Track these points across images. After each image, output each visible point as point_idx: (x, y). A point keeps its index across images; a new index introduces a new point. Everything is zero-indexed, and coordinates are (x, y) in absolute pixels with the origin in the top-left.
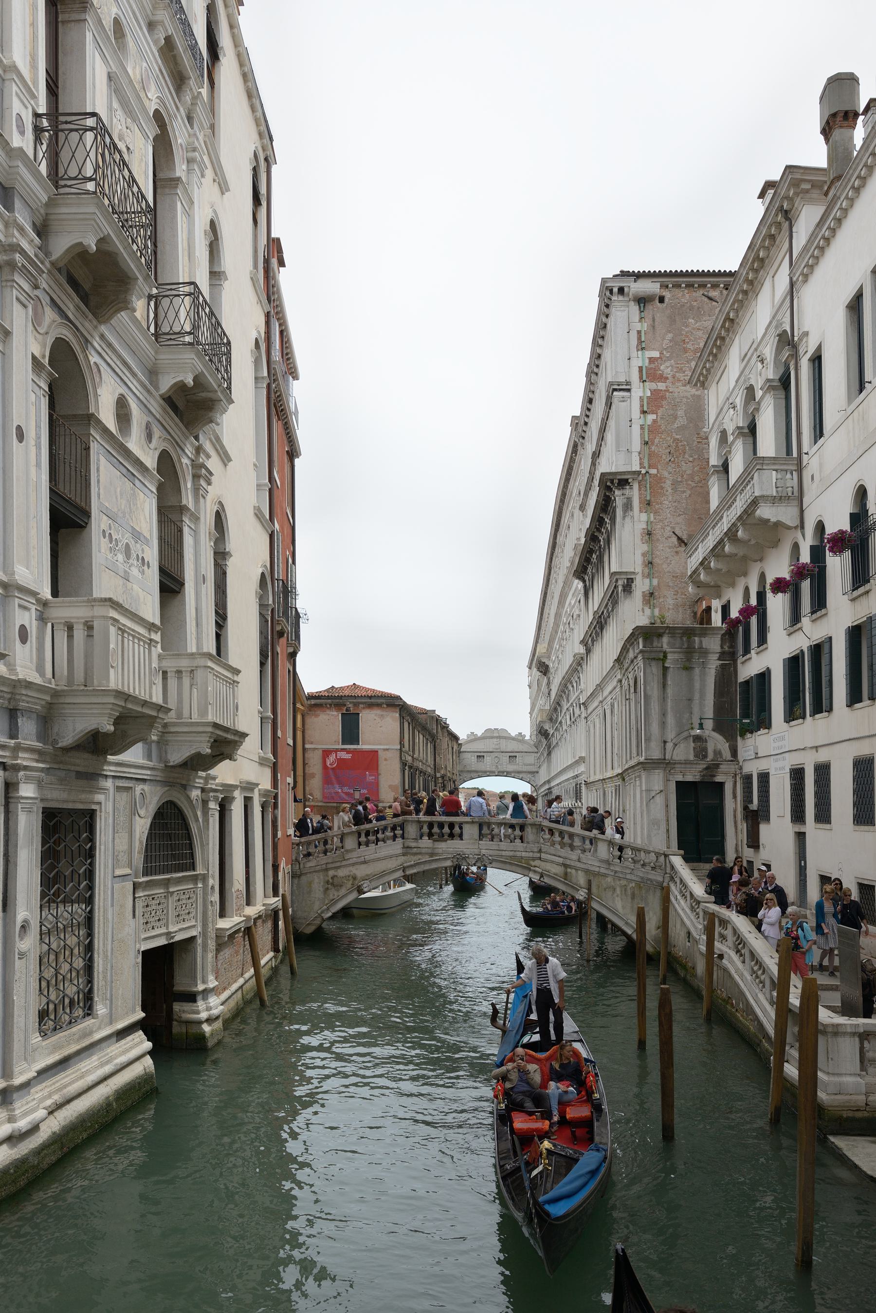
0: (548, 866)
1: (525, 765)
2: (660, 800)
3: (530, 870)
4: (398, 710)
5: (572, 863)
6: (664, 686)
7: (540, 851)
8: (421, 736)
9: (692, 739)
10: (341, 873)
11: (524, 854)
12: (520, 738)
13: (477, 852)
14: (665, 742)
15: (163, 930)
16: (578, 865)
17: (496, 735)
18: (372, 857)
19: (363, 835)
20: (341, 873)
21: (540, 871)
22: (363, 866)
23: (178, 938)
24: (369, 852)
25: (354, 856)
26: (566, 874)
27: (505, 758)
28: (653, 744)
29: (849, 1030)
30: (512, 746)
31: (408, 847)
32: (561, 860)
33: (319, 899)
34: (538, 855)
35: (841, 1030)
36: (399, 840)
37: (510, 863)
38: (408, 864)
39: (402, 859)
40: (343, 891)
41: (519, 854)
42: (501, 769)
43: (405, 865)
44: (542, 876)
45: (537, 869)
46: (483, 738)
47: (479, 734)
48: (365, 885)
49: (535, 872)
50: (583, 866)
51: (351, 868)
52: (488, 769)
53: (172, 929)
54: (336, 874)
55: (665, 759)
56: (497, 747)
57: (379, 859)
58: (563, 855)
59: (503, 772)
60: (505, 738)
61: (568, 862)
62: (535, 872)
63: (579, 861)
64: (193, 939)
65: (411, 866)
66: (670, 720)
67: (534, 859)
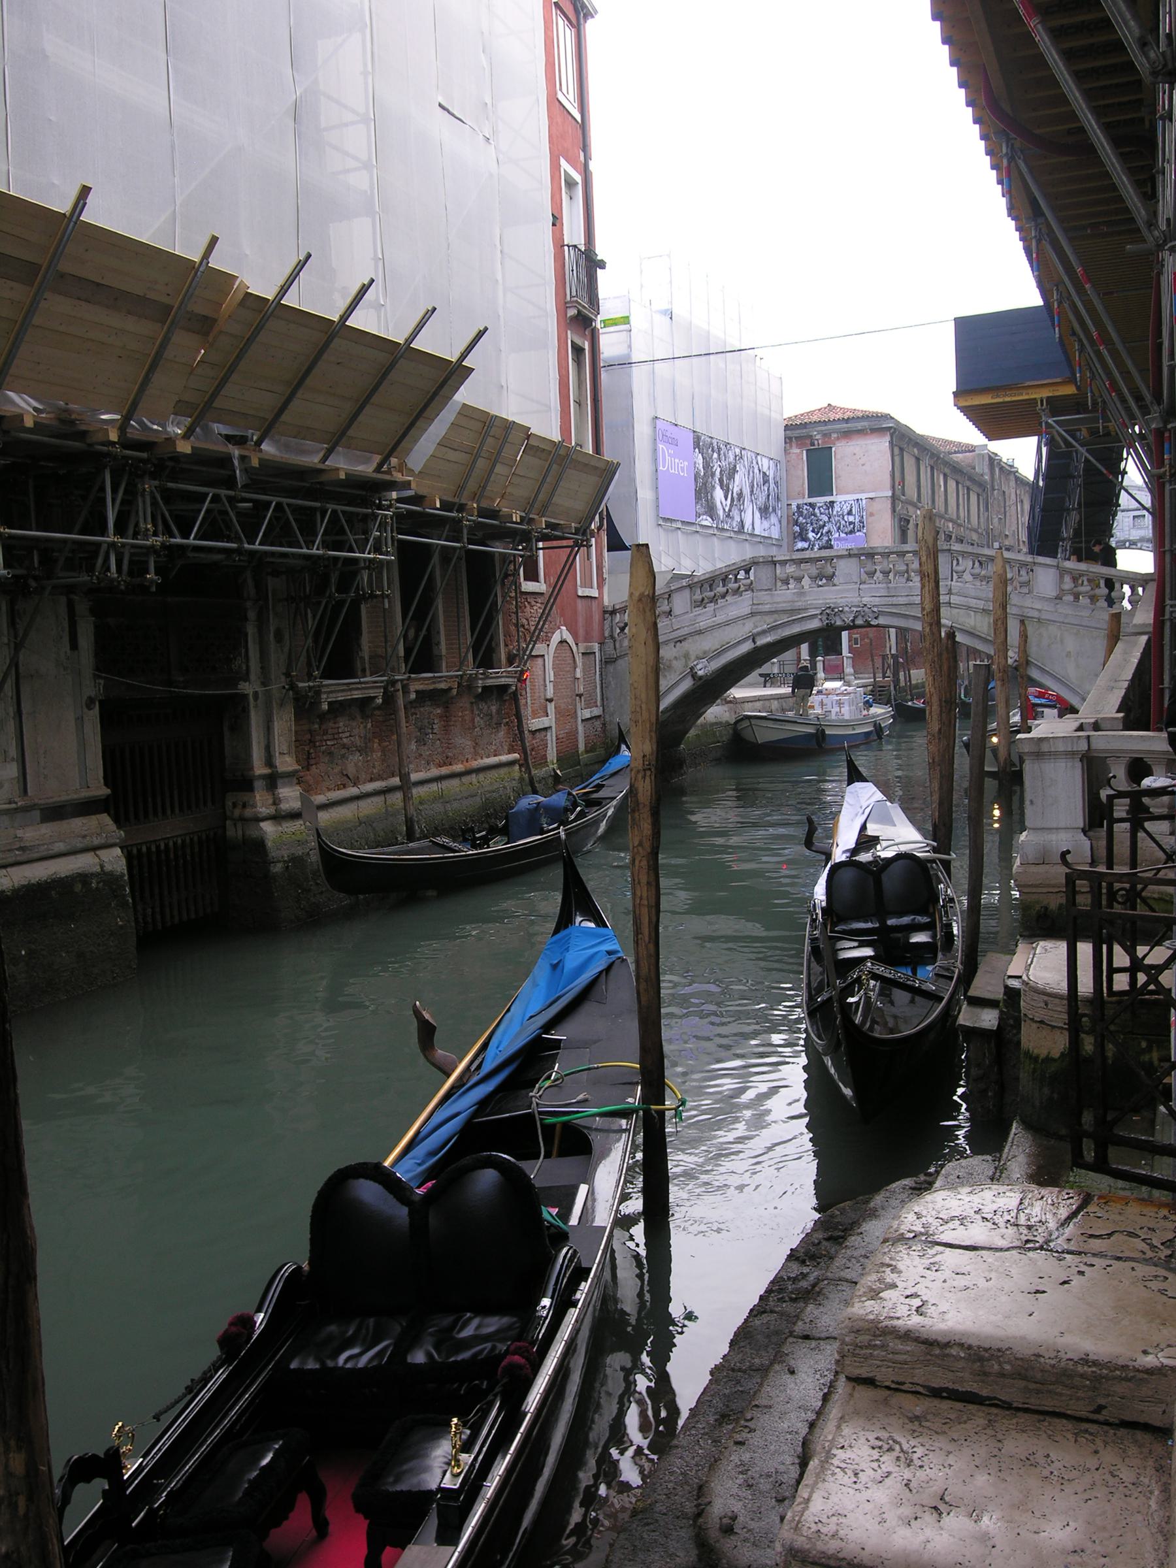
4: (888, 438)
8: (952, 484)
13: (856, 601)
18: (710, 622)
29: (1061, 748)
35: (1045, 748)
38: (759, 629)
43: (755, 631)
48: (699, 667)
57: (720, 626)
65: (764, 632)
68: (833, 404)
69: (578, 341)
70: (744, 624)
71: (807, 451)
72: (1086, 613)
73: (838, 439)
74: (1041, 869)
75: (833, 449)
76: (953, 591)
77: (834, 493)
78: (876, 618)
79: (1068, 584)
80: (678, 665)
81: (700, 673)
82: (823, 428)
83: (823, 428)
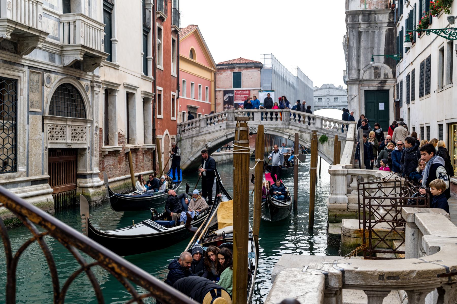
1: (342, 102)
2: (356, 100)
3: (284, 134)
6: (359, 42)
7: (289, 124)
9: (373, 68)
11: (281, 126)
12: (340, 88)
14: (359, 70)
17: (328, 87)
18: (213, 130)
19: (209, 120)
20: (200, 138)
21: (288, 134)
22: (208, 135)
24: (211, 128)
25: (204, 131)
27: (332, 99)
28: (353, 72)
30: (336, 93)
33: (189, 152)
34: (287, 127)
35: (337, 173)
36: (225, 122)
37: (275, 131)
39: (226, 131)
41: (279, 126)
42: (330, 104)
43: (227, 134)
44: (289, 136)
46: (321, 89)
47: (320, 87)
48: (209, 144)
49: (286, 135)
51: (203, 136)
52: (324, 105)
54: (197, 139)
55: (359, 79)
56: (328, 93)
57: (215, 131)
58: (299, 126)
59: (331, 106)
60: (333, 88)
62: (286, 135)
63: (307, 129)
64: (85, 149)
65: (230, 134)
66: (362, 59)
67: (286, 129)
68: (242, 57)
69: (174, 38)
71: (234, 73)
73: (244, 69)
74: (335, 204)
75: (242, 73)
77: (242, 87)
78: (266, 131)
80: (202, 144)
81: (209, 146)
82: (239, 66)
83: (239, 66)
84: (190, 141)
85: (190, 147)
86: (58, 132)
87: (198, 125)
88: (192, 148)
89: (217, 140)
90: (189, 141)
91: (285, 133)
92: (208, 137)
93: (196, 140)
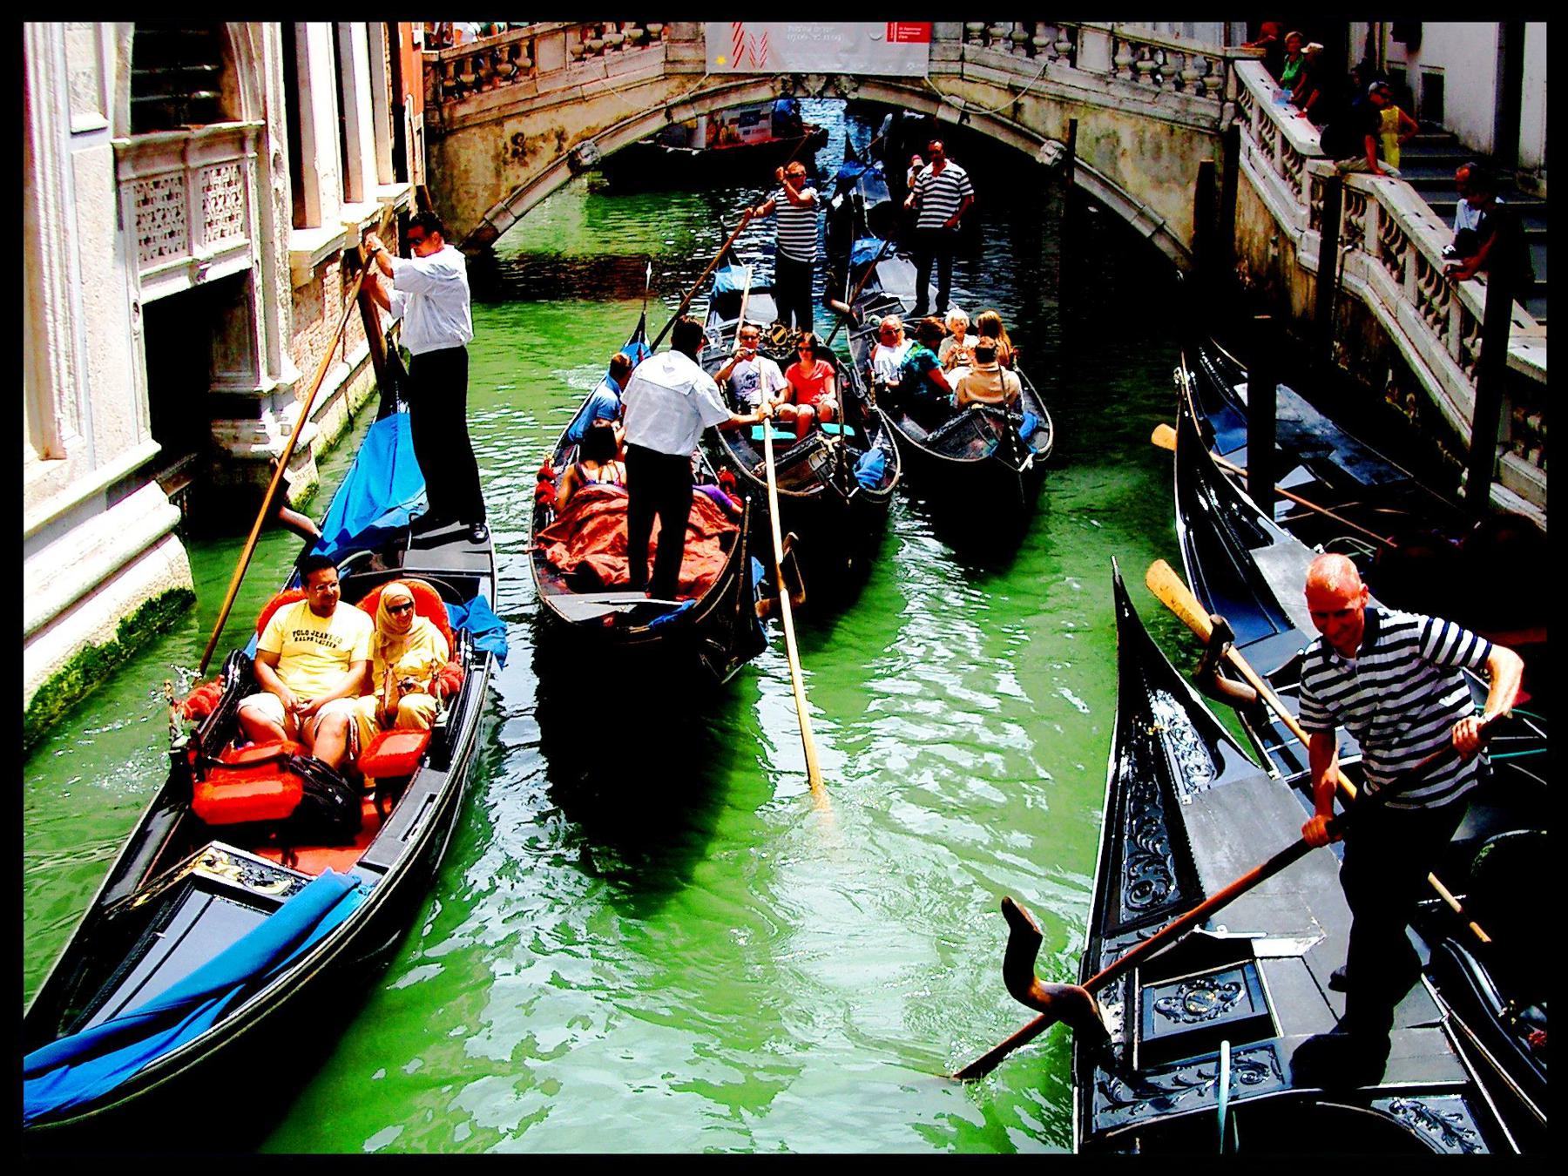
0: (978, 93)
5: (1027, 84)
10: (532, 127)
15: (182, 258)
16: (1042, 86)
18: (597, 87)
21: (959, 102)
23: (214, 273)
26: (1017, 107)
31: (674, 62)
32: (1006, 79)
34: (956, 68)
38: (678, 99)
40: (537, 166)
43: (671, 102)
44: (964, 115)
45: (954, 100)
48: (585, 152)
50: (1052, 89)
51: (553, 114)
53: (200, 253)
54: (520, 129)
61: (1019, 82)
64: (244, 276)
65: (684, 103)
67: (948, 75)
70: (652, 91)
72: (1148, 98)
76: (967, 57)
79: (1124, 57)
80: (548, 151)
84: (491, 138)
85: (492, 165)
86: (161, 213)
87: (524, 61)
88: (498, 174)
89: (621, 130)
90: (484, 139)
91: (944, 98)
92: (575, 121)
93: (522, 135)
